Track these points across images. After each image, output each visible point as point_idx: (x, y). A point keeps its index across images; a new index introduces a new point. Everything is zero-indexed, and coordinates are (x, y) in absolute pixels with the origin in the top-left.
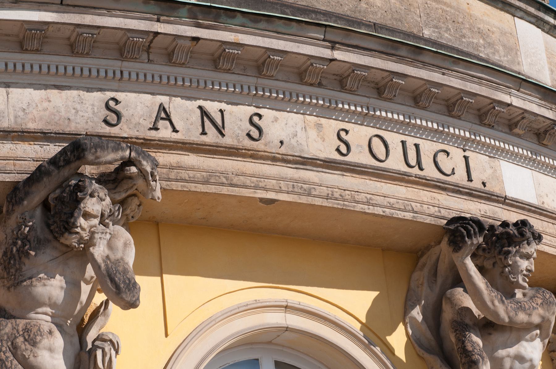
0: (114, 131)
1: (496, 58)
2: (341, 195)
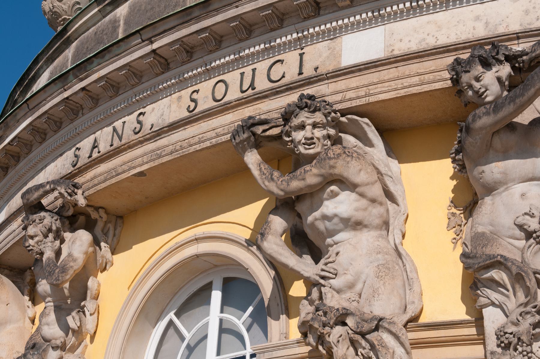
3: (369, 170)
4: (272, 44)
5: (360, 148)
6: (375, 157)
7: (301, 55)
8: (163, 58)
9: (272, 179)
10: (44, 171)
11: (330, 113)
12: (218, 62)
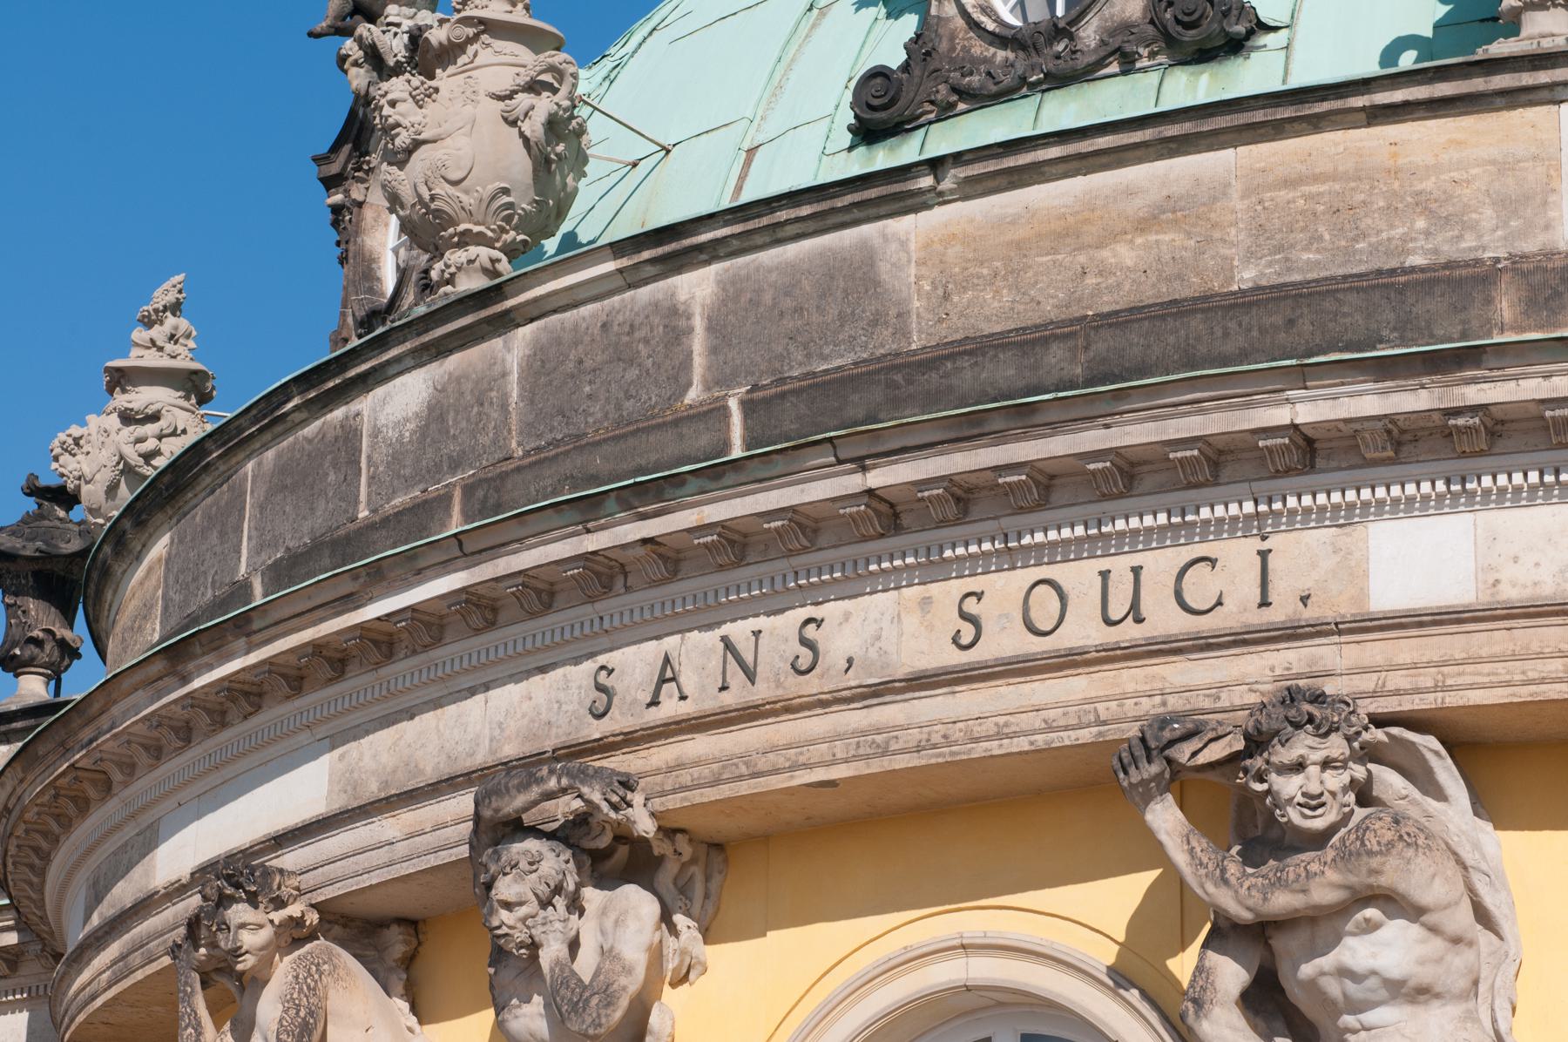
2: (945, 737)
3: (1449, 873)
4: (1189, 518)
5: (1414, 802)
6: (1451, 826)
7: (1264, 555)
8: (886, 501)
9: (1226, 882)
10: (479, 698)
11: (1358, 733)
12: (1039, 537)
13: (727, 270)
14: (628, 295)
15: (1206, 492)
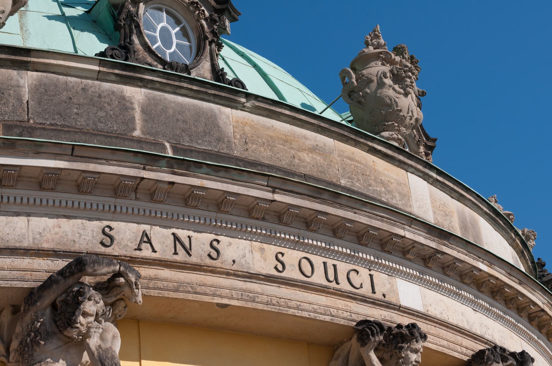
0: (108, 251)
1: (393, 202)
2: (277, 302)
13: (150, 94)
14: (97, 82)
15: (364, 248)
